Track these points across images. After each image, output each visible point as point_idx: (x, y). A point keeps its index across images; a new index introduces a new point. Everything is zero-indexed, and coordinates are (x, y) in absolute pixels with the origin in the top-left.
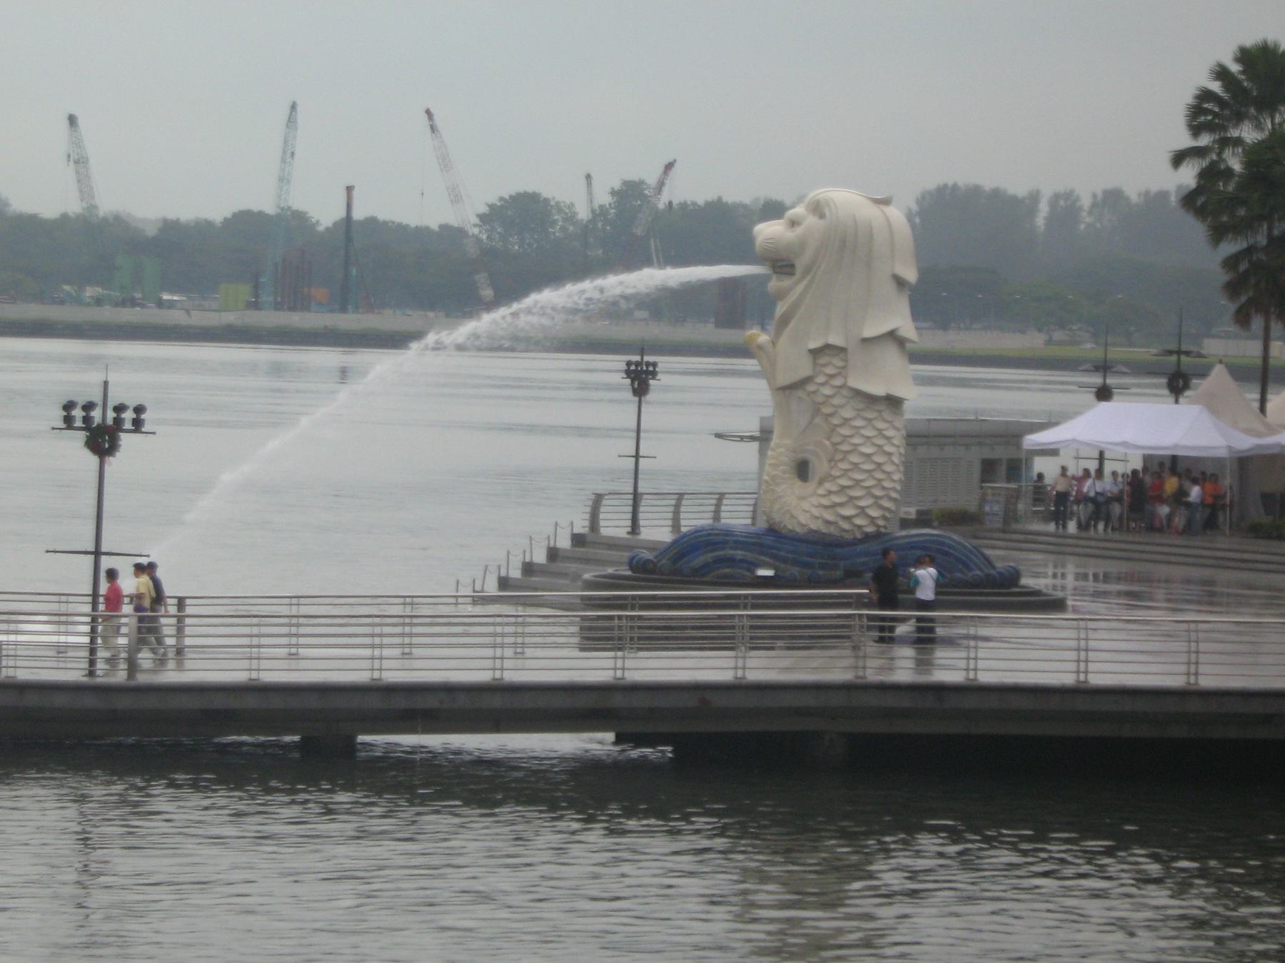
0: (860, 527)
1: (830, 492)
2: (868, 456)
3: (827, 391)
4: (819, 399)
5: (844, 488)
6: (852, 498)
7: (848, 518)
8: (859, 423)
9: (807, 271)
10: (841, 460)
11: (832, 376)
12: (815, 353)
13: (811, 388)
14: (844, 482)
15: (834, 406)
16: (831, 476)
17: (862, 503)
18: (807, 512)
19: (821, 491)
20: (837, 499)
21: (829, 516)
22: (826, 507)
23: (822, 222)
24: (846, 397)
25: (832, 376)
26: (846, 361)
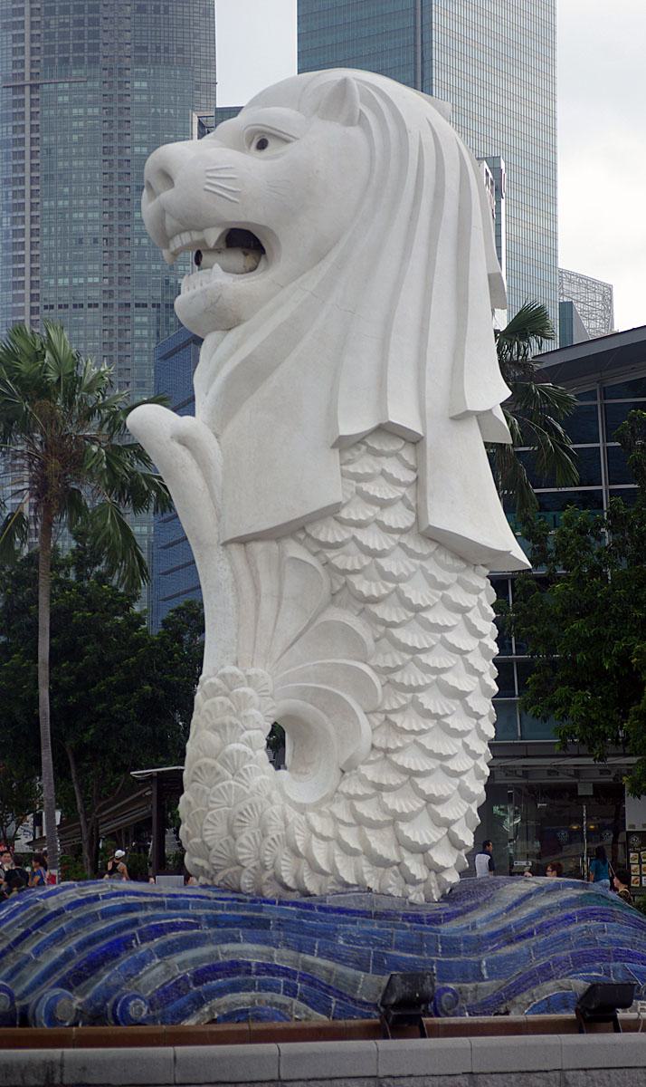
0: (438, 870)
1: (380, 788)
2: (461, 695)
3: (373, 539)
6: (431, 800)
7: (422, 850)
9: (319, 255)
10: (403, 709)
11: (384, 504)
12: (344, 445)
13: (329, 533)
14: (410, 760)
15: (387, 576)
16: (373, 746)
19: (352, 787)
20: (395, 803)
21: (382, 845)
24: (411, 554)
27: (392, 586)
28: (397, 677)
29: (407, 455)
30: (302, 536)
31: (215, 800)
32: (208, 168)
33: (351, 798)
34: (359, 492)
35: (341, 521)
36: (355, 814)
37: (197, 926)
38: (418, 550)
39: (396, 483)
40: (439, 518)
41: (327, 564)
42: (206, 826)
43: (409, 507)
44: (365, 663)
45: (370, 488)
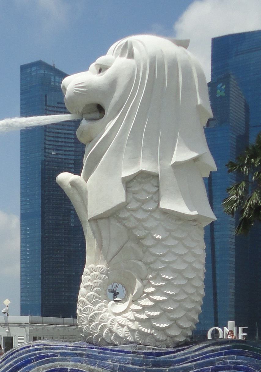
0: (172, 337)
1: (145, 308)
3: (140, 215)
4: (132, 223)
5: (157, 302)
6: (165, 311)
8: (171, 242)
11: (144, 202)
15: (146, 229)
17: (175, 316)
18: (123, 326)
22: (141, 321)
23: (132, 62)
24: (156, 219)
25: (144, 202)
26: (158, 187)
27: (147, 232)
28: (152, 266)
29: (154, 182)
30: (115, 216)
31: (84, 312)
32: (76, 84)
33: (133, 310)
34: (134, 197)
35: (129, 210)
36: (135, 317)
37: (57, 356)
38: (158, 217)
39: (149, 193)
40: (165, 205)
41: (124, 225)
42: (81, 322)
43: (155, 202)
44: (141, 261)
45: (139, 197)
